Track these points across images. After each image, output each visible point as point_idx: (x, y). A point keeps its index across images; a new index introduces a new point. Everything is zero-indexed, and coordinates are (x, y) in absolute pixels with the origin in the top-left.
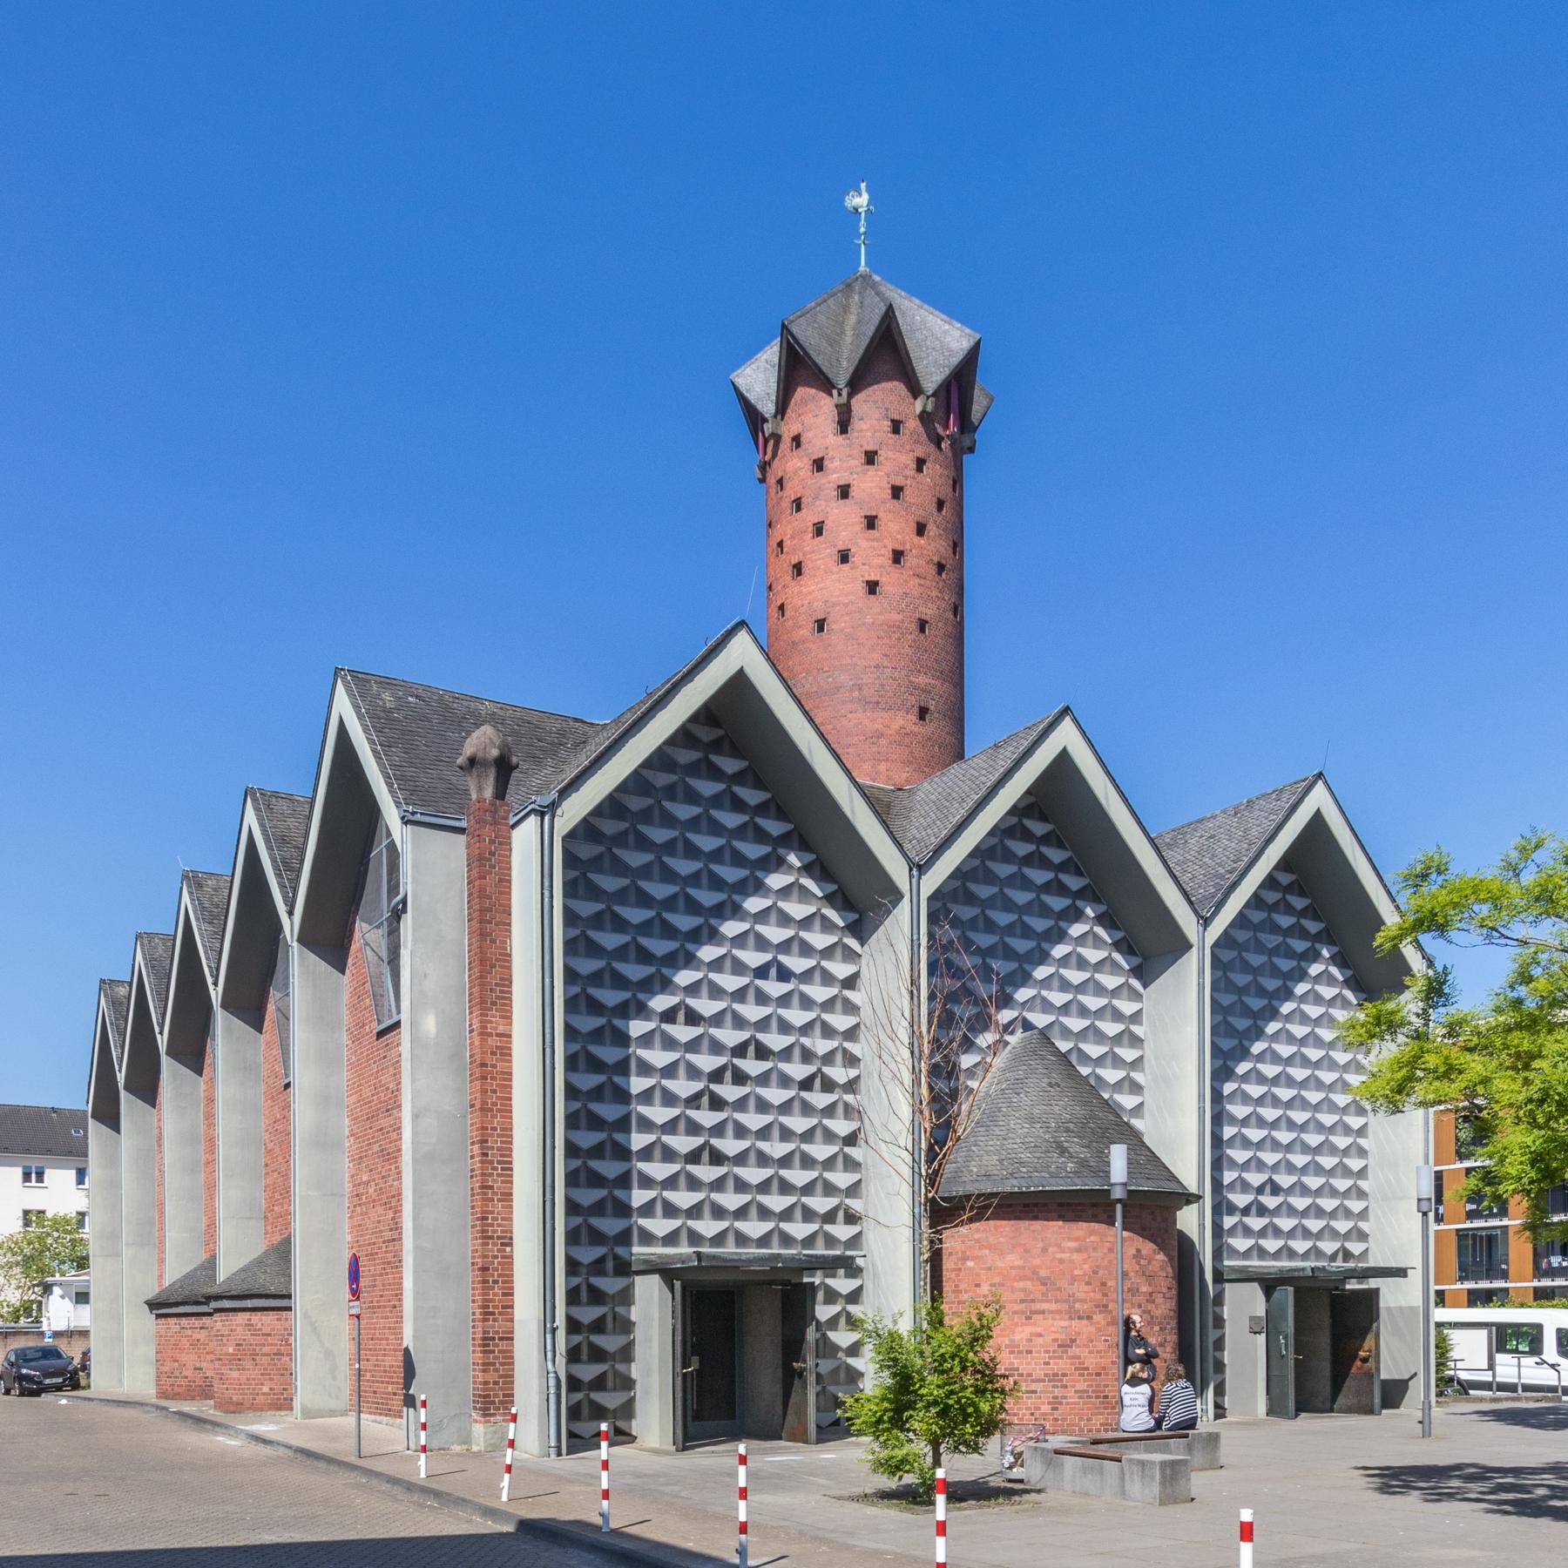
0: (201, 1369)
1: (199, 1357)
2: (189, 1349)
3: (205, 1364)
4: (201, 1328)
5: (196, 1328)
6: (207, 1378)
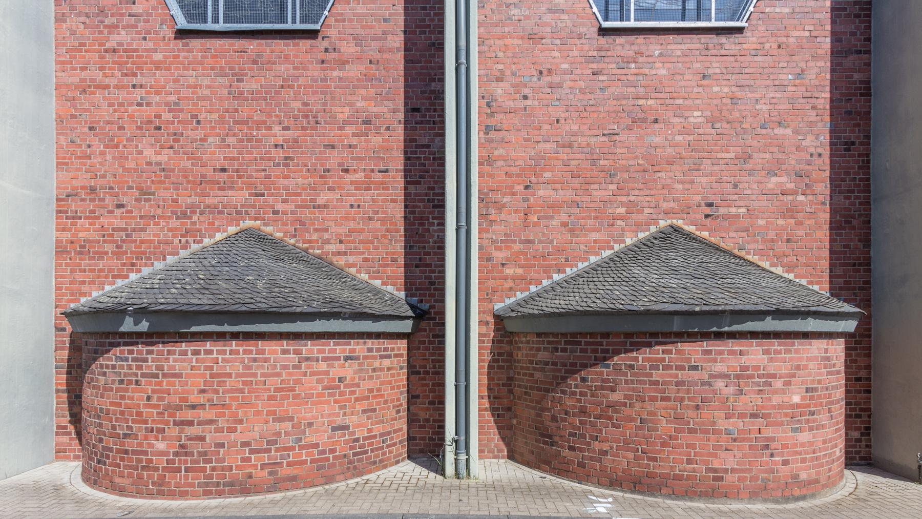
0: (346, 428)
1: (341, 408)
2: (319, 395)
3: (355, 418)
4: (347, 359)
5: (338, 359)
6: (357, 440)
